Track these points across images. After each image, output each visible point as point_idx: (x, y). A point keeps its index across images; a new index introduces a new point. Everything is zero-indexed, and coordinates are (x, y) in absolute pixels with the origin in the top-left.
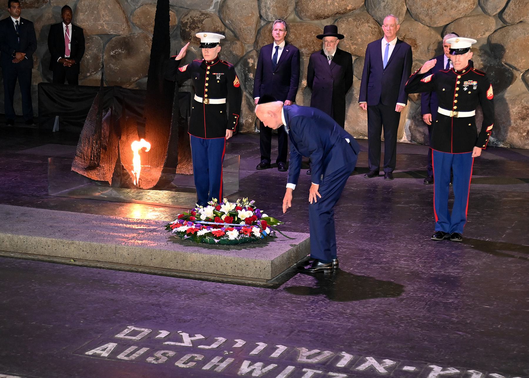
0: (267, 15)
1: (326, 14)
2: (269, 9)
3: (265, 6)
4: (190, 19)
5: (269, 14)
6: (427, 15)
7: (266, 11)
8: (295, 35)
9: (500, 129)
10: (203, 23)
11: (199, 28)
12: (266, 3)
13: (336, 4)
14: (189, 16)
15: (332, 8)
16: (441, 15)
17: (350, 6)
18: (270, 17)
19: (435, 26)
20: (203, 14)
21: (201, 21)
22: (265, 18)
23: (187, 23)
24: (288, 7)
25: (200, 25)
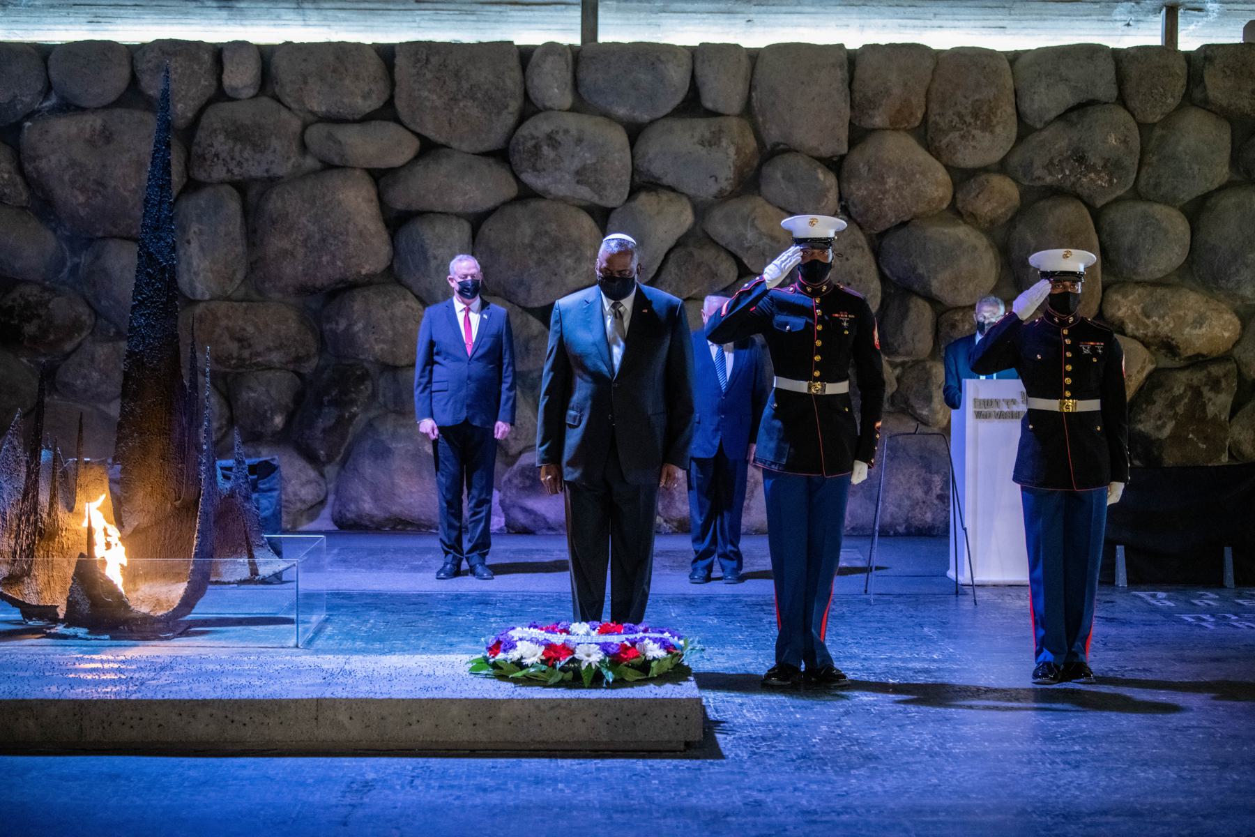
0: (193, 288)
1: (318, 284)
2: (197, 274)
3: (189, 271)
4: (19, 300)
5: (197, 284)
6: (521, 283)
7: (191, 283)
8: (256, 326)
9: (672, 498)
10: (50, 306)
11: (39, 316)
12: (190, 264)
13: (339, 263)
14: (15, 294)
15: (330, 271)
16: (548, 283)
17: (367, 267)
18: (199, 292)
19: (536, 305)
20: (45, 289)
21: (45, 304)
22: (188, 294)
23: (12, 308)
24: (234, 272)
25: (42, 312)
